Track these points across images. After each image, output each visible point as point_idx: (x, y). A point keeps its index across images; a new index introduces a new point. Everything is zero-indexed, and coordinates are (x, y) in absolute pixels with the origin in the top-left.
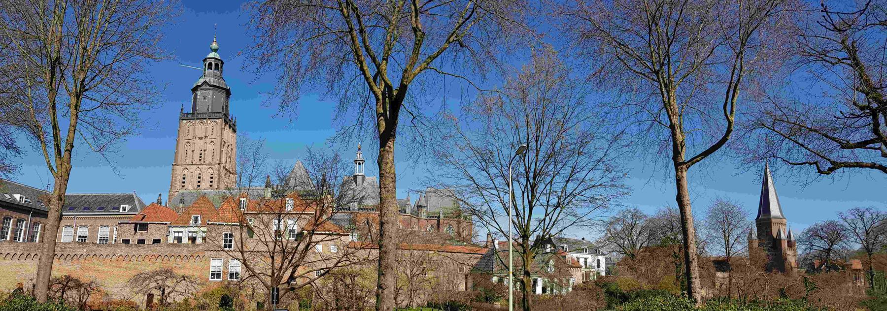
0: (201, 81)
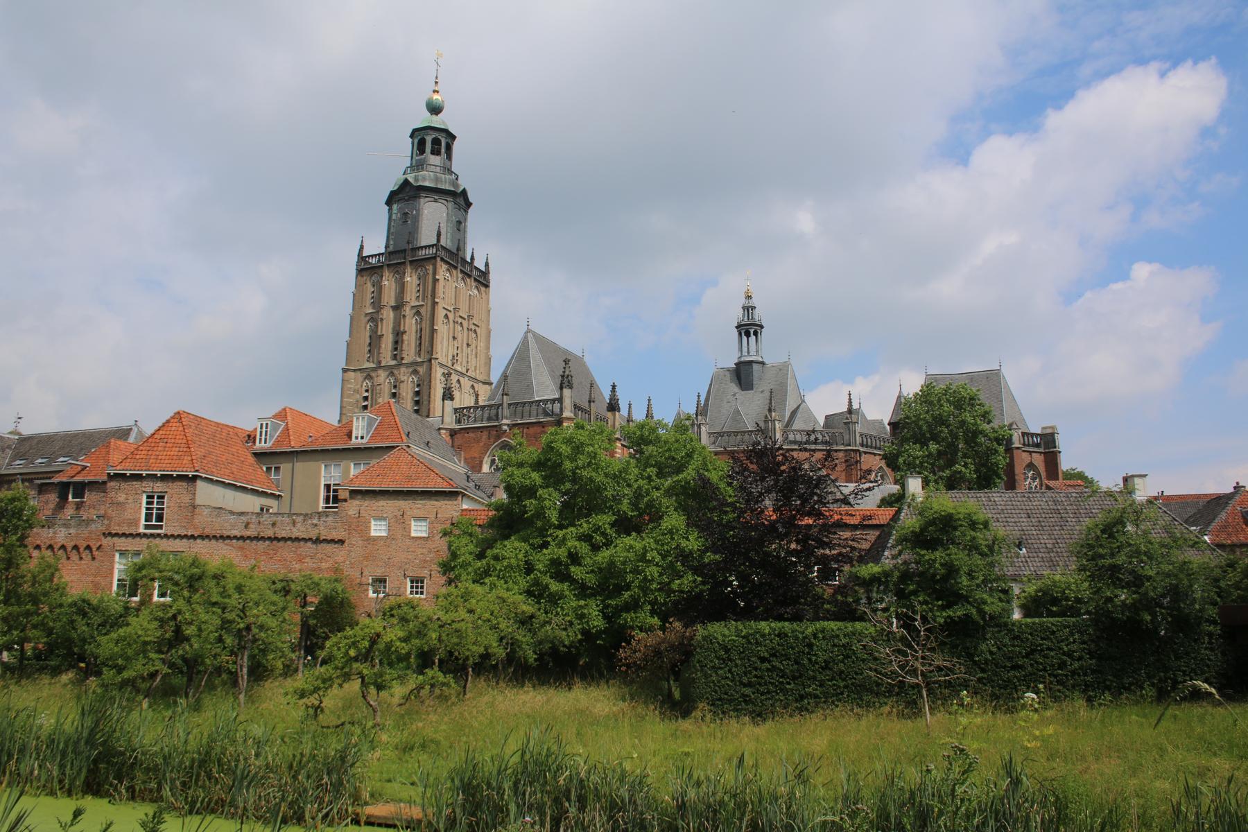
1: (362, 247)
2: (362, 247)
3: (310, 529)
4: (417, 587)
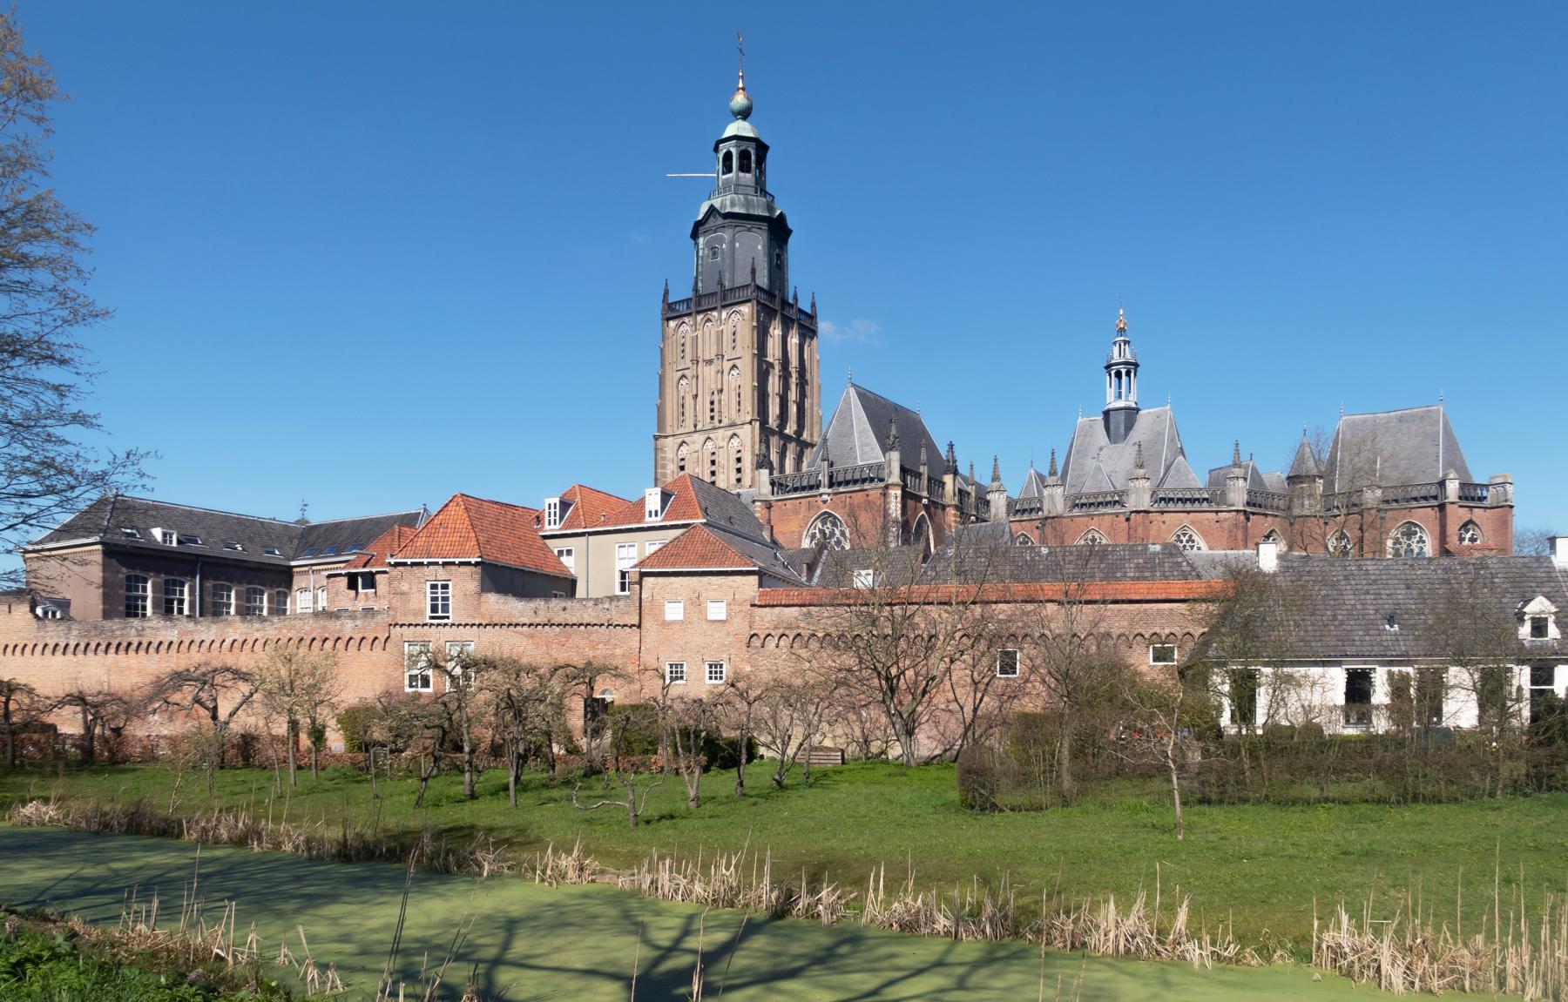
0: (704, 208)
1: (666, 292)
2: (666, 292)
3: (601, 614)
4: (716, 672)
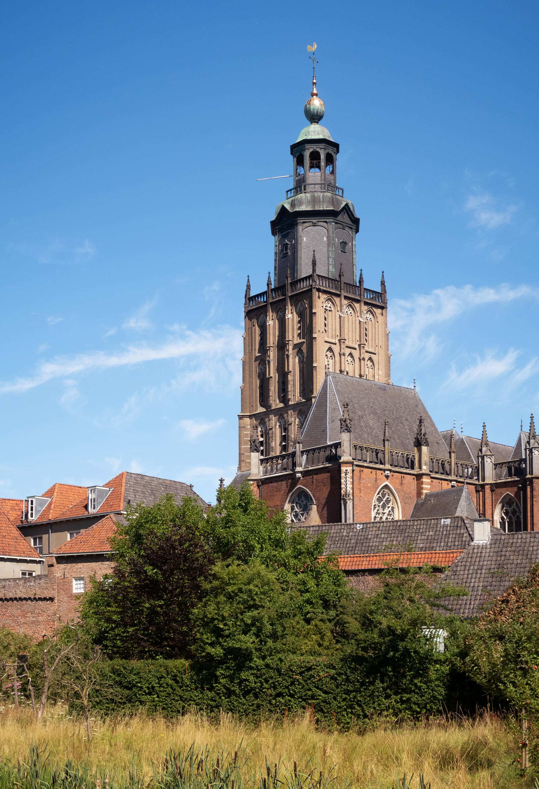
1: (248, 287)
2: (248, 287)
